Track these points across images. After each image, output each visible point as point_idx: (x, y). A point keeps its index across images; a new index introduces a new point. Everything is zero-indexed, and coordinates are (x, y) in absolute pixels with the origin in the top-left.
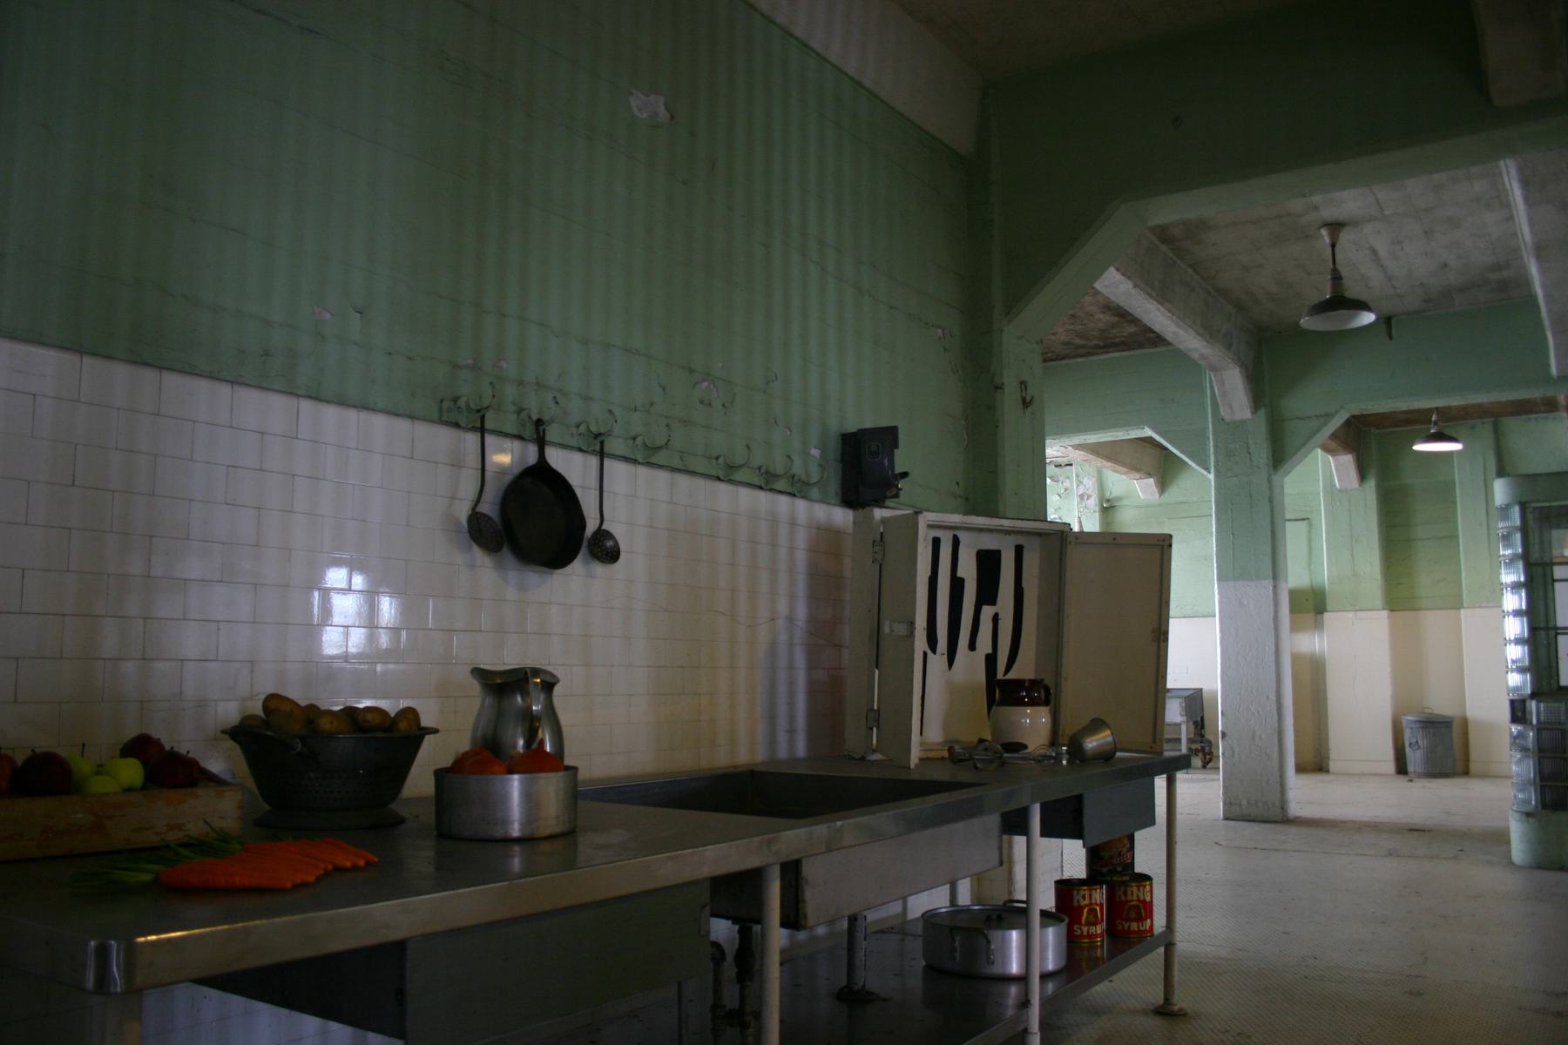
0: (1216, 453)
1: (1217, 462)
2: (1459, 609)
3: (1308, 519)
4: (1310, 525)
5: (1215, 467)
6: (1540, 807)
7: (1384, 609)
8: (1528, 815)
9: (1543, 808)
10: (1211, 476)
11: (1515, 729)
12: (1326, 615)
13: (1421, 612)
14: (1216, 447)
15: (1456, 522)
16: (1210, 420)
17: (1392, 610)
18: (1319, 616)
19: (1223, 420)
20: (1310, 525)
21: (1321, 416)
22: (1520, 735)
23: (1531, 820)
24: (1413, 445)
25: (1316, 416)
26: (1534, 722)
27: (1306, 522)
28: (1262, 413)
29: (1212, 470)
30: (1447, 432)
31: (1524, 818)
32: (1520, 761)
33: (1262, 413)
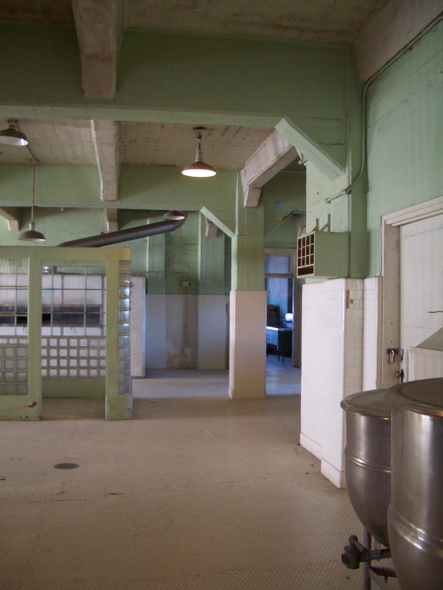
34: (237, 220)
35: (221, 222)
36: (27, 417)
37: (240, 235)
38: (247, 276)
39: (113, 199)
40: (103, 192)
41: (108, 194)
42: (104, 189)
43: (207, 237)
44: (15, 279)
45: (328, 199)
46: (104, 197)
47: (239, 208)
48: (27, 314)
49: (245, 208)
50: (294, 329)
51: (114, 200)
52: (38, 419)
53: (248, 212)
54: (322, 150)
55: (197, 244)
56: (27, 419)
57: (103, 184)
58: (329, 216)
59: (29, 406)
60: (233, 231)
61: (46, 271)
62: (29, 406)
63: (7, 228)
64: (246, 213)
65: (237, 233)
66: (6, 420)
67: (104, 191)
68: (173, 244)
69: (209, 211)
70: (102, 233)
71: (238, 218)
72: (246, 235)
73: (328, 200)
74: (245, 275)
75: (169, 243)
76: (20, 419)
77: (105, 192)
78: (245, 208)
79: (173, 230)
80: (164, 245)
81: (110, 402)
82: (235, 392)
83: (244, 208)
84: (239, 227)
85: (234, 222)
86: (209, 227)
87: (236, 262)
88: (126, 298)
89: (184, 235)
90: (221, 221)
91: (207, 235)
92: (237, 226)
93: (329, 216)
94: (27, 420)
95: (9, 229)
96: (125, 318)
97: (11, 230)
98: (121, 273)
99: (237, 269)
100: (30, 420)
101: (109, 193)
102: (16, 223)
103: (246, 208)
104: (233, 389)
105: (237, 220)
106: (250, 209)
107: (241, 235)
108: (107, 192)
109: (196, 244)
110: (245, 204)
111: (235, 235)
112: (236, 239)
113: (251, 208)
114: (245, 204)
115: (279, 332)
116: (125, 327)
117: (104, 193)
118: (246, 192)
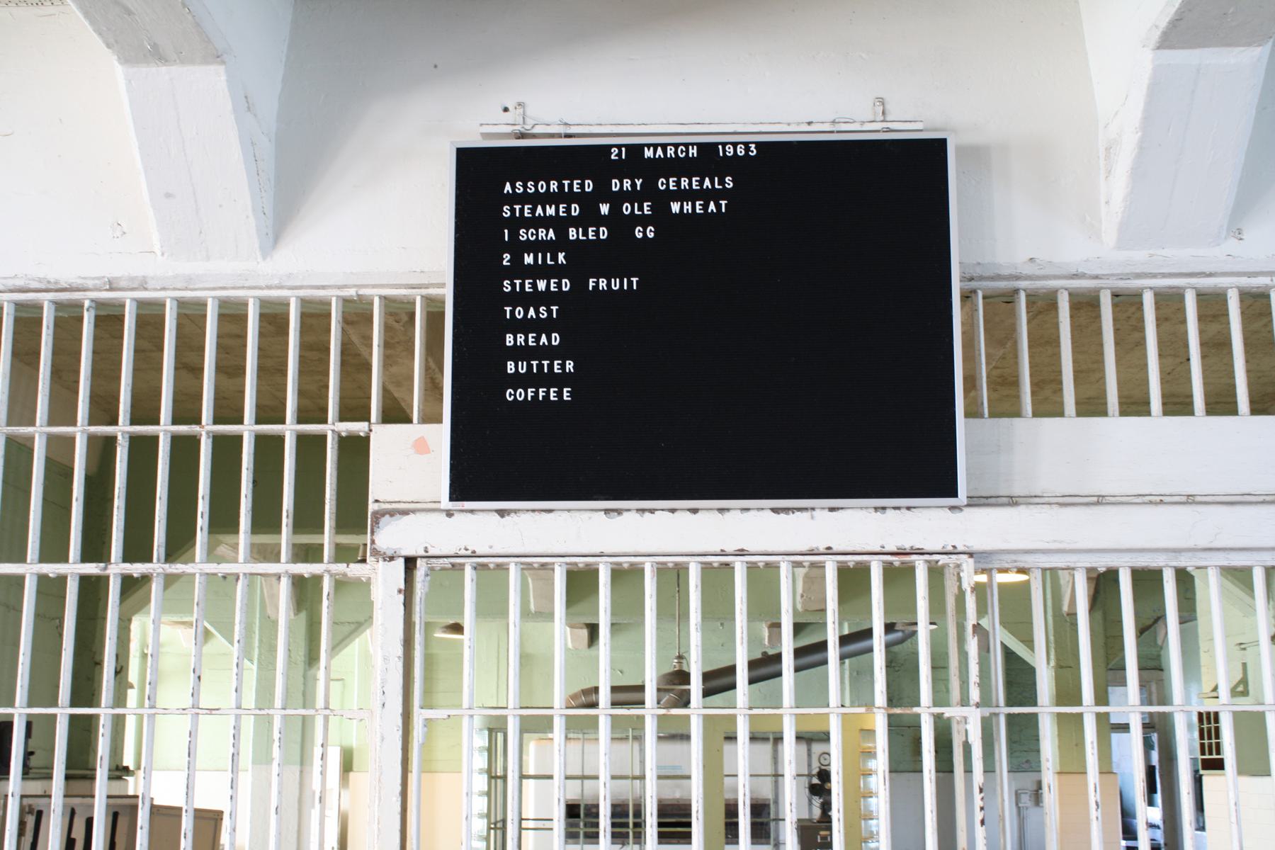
0: (260, 647)
1: (260, 655)
3: (342, 680)
4: (344, 686)
5: (258, 659)
10: (255, 667)
12: (352, 775)
13: (437, 774)
14: (261, 641)
16: (258, 615)
18: (346, 773)
19: (269, 617)
20: (344, 686)
21: (353, 623)
25: (349, 623)
27: (341, 682)
28: (303, 615)
29: (256, 662)
33: (303, 615)
35: (1021, 644)
40: (802, 596)
41: (810, 598)
42: (804, 591)
44: (581, 748)
45: (1241, 644)
46: (803, 604)
49: (1065, 615)
50: (1165, 844)
54: (1230, 578)
57: (804, 582)
58: (1244, 665)
64: (1068, 624)
67: (805, 595)
68: (897, 669)
70: (765, 653)
71: (1054, 636)
72: (1070, 667)
73: (1243, 646)
77: (807, 597)
78: (1065, 615)
83: (1063, 615)
84: (1056, 651)
90: (1022, 641)
93: (1244, 665)
97: (573, 647)
99: (1056, 733)
101: (813, 598)
103: (1068, 615)
107: (1061, 667)
108: (809, 596)
117: (805, 597)
118: (1068, 587)
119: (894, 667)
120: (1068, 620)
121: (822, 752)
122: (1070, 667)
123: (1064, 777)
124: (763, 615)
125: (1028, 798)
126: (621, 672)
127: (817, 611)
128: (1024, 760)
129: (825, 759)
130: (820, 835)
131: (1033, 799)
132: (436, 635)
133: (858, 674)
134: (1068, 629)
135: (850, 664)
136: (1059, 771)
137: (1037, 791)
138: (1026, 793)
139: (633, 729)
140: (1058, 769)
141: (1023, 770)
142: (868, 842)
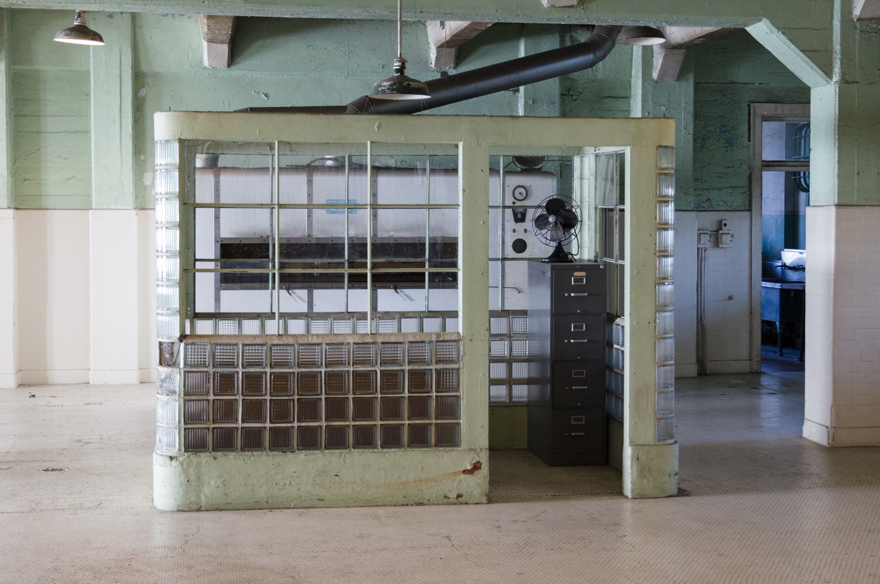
2: (89, 209)
6: (183, 449)
7: (8, 208)
8: (171, 458)
9: (185, 451)
11: (164, 370)
13: (49, 211)
15: (88, 116)
17: (17, 209)
22: (169, 377)
23: (174, 463)
24: (54, 38)
26: (182, 365)
30: (92, 27)
31: (168, 460)
32: (167, 403)
34: (837, 47)
35: (801, 53)
36: (459, 496)
37: (845, 82)
38: (858, 173)
39: (570, 4)
43: (656, 82)
47: (843, 21)
48: (455, 265)
49: (855, 21)
51: (572, 7)
52: (484, 500)
53: (862, 31)
55: (627, 98)
56: (460, 499)
59: (465, 472)
60: (828, 73)
61: (329, 163)
62: (465, 472)
63: (202, 62)
65: (836, 77)
66: (412, 505)
68: (575, 98)
69: (775, 30)
71: (841, 45)
72: (857, 83)
74: (856, 172)
75: (564, 95)
76: (446, 501)
78: (855, 21)
79: (592, 65)
80: (557, 98)
81: (638, 459)
82: (835, 429)
83: (853, 21)
84: (842, 64)
85: (829, 52)
86: (665, 59)
87: (835, 143)
88: (666, 229)
89: (600, 76)
90: (802, 51)
91: (655, 75)
92: (839, 62)
94: (461, 503)
95: (206, 63)
96: (666, 272)
97: (209, 65)
98: (660, 174)
99: (837, 159)
100: (466, 503)
102: (224, 49)
103: (858, 20)
104: (828, 425)
105: (837, 47)
106: (866, 23)
107: (847, 82)
109: (626, 98)
110: (857, 12)
111: (832, 83)
112: (835, 91)
113: (870, 19)
114: (857, 12)
115: (782, 291)
116: (665, 293)
119: (572, 95)
120: (858, 27)
121: (515, 185)
122: (857, 83)
123: (844, 210)
124: (500, 11)
125: (708, 238)
126: (266, 95)
127: (566, 7)
128: (705, 199)
129: (520, 193)
130: (574, 276)
131: (712, 239)
132: (56, 40)
133: (533, 102)
134: (858, 37)
135: (525, 90)
136: (836, 204)
137: (717, 231)
138: (707, 233)
139: (370, 143)
140: (836, 202)
141: (703, 209)
142: (664, 284)
